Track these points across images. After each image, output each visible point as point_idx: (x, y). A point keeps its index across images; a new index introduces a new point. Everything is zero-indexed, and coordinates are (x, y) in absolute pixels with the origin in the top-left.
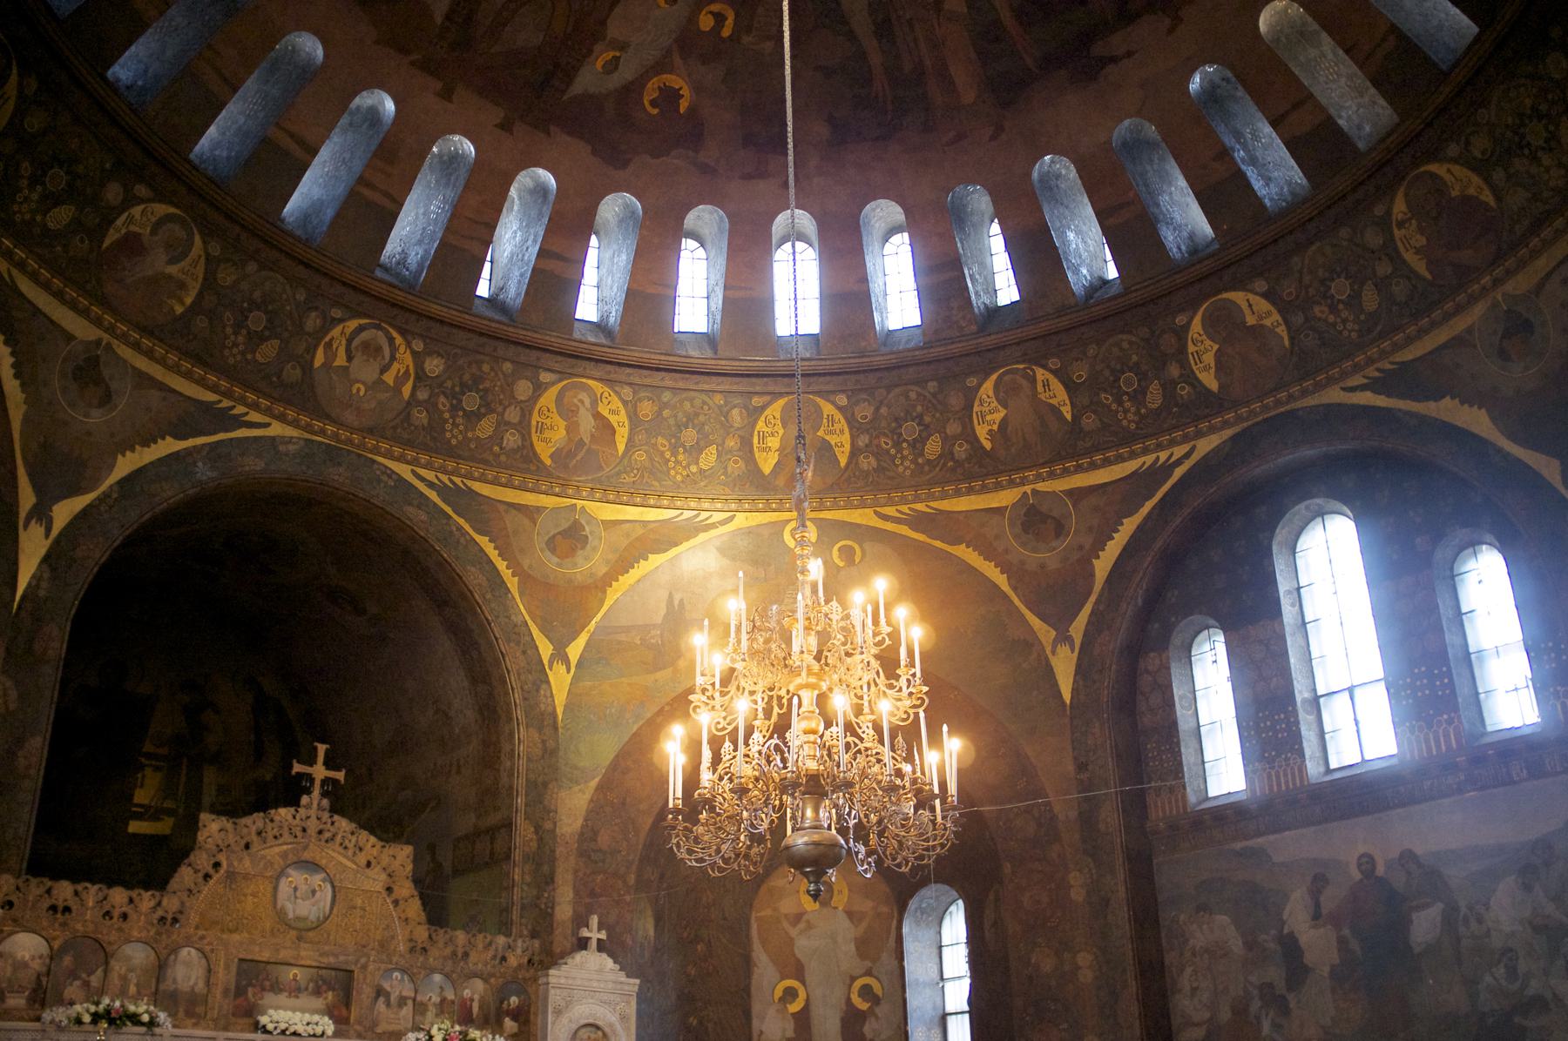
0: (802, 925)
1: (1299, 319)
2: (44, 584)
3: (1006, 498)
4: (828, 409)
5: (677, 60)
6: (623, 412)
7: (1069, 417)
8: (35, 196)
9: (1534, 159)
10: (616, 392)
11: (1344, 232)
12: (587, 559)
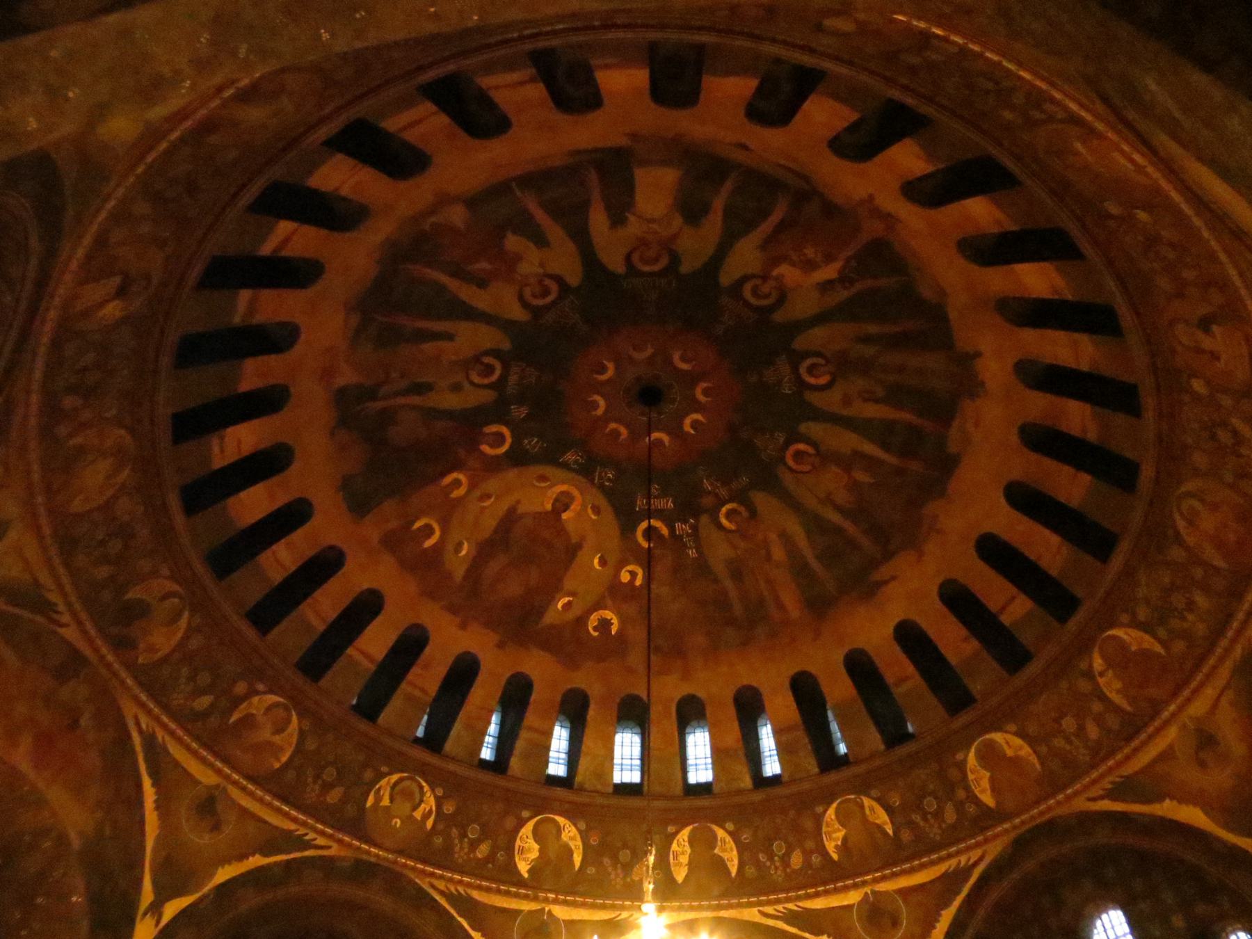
1: (1044, 749)
3: (853, 897)
4: (721, 833)
5: (609, 602)
7: (890, 832)
9: (1183, 619)
10: (575, 825)
11: (1064, 685)
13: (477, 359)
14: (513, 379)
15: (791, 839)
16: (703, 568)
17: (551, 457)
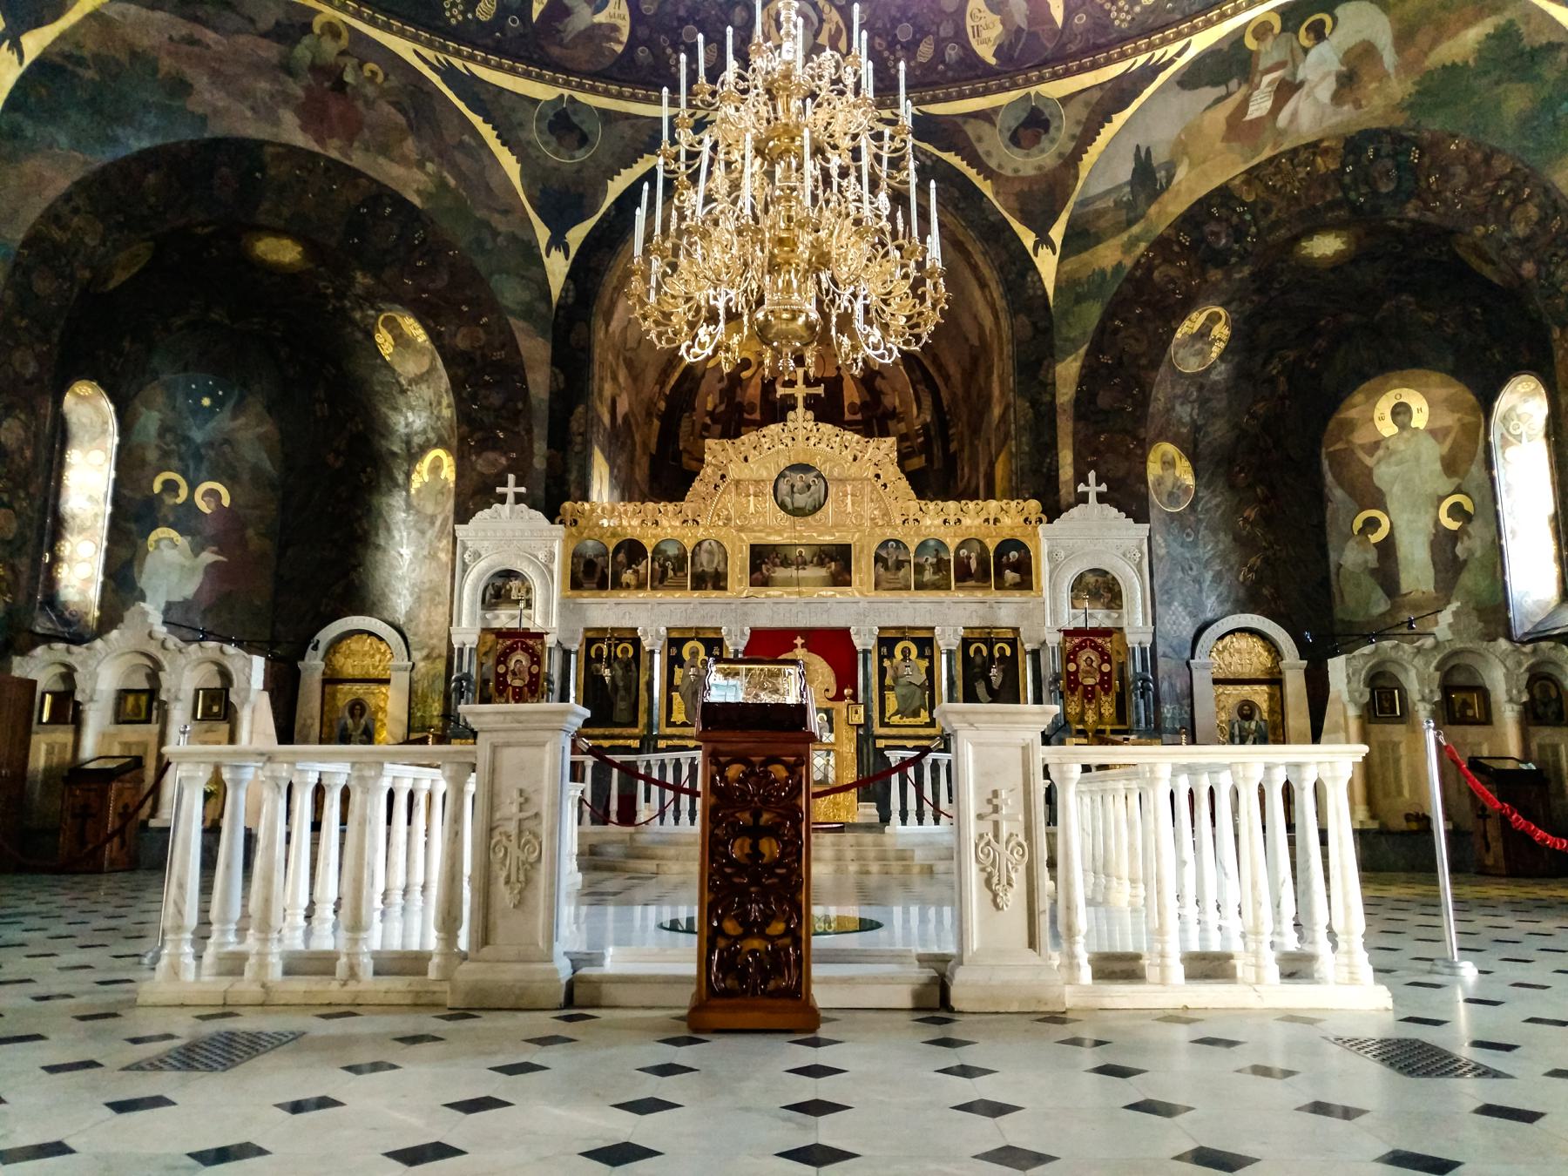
0: (1380, 453)
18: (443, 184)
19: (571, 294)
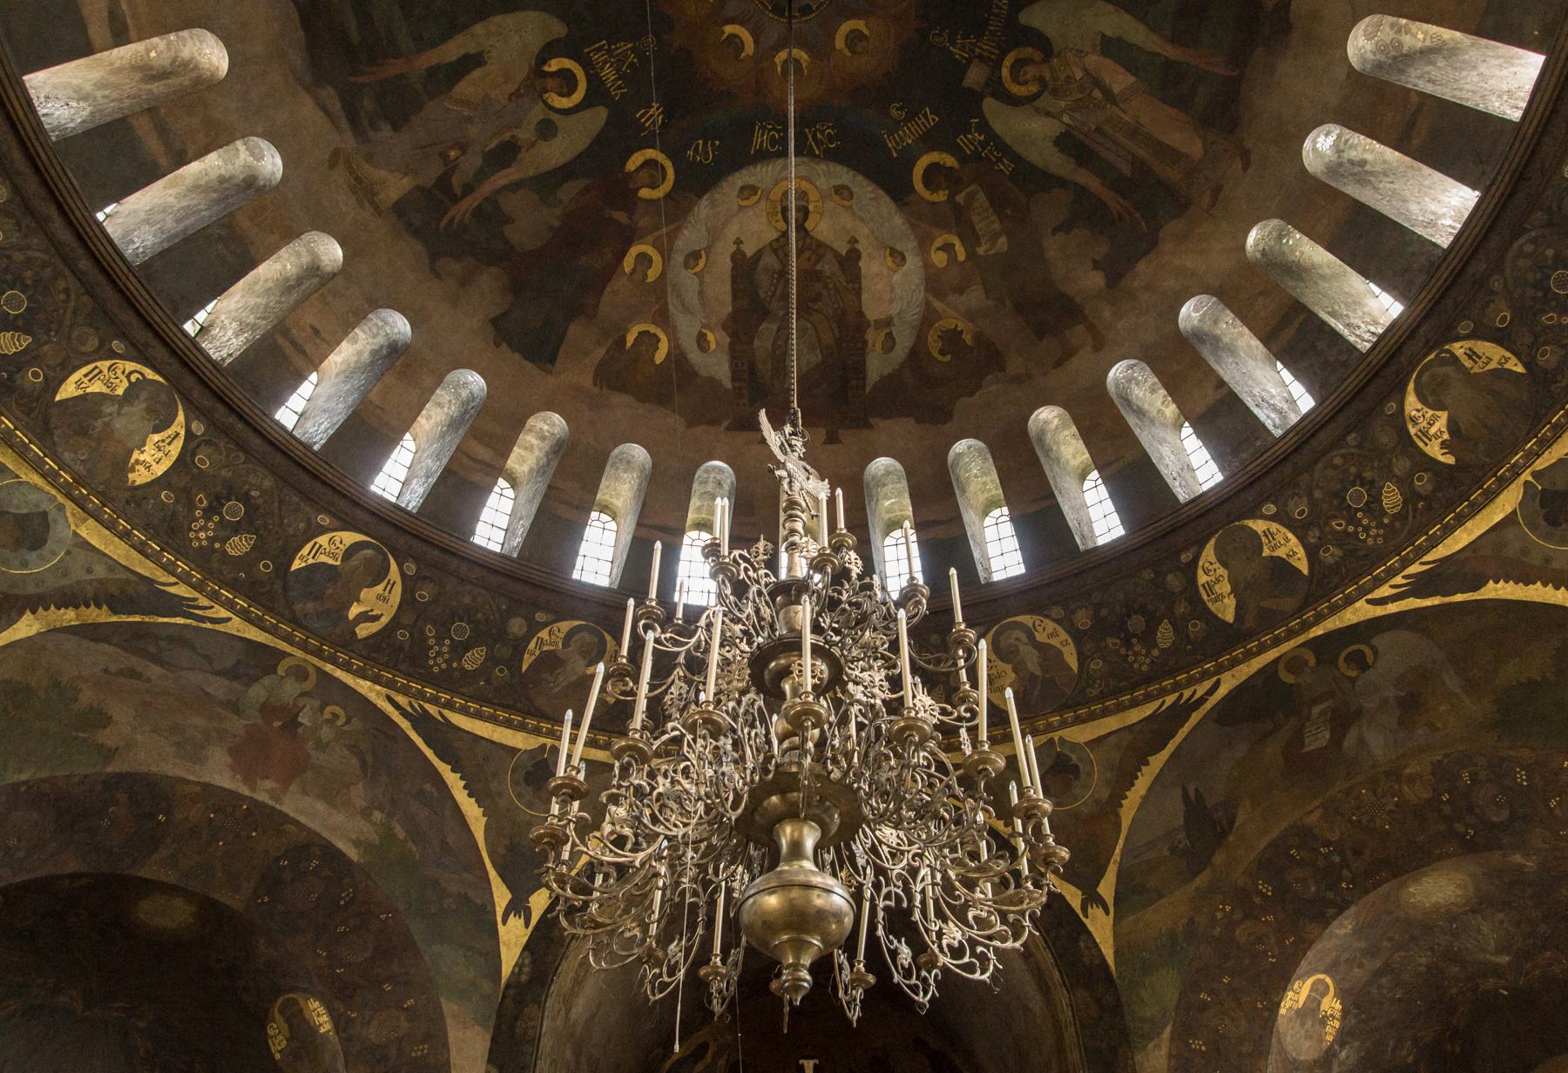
2: (526, 969)
3: (1508, 502)
4: (1259, 526)
6: (1060, 629)
7: (1520, 369)
8: (445, 649)
10: (1047, 616)
12: (1086, 787)
13: (538, 73)
14: (608, 73)
15: (1368, 475)
16: (1033, 178)
17: (737, 155)
18: (388, 835)
19: (526, 969)
